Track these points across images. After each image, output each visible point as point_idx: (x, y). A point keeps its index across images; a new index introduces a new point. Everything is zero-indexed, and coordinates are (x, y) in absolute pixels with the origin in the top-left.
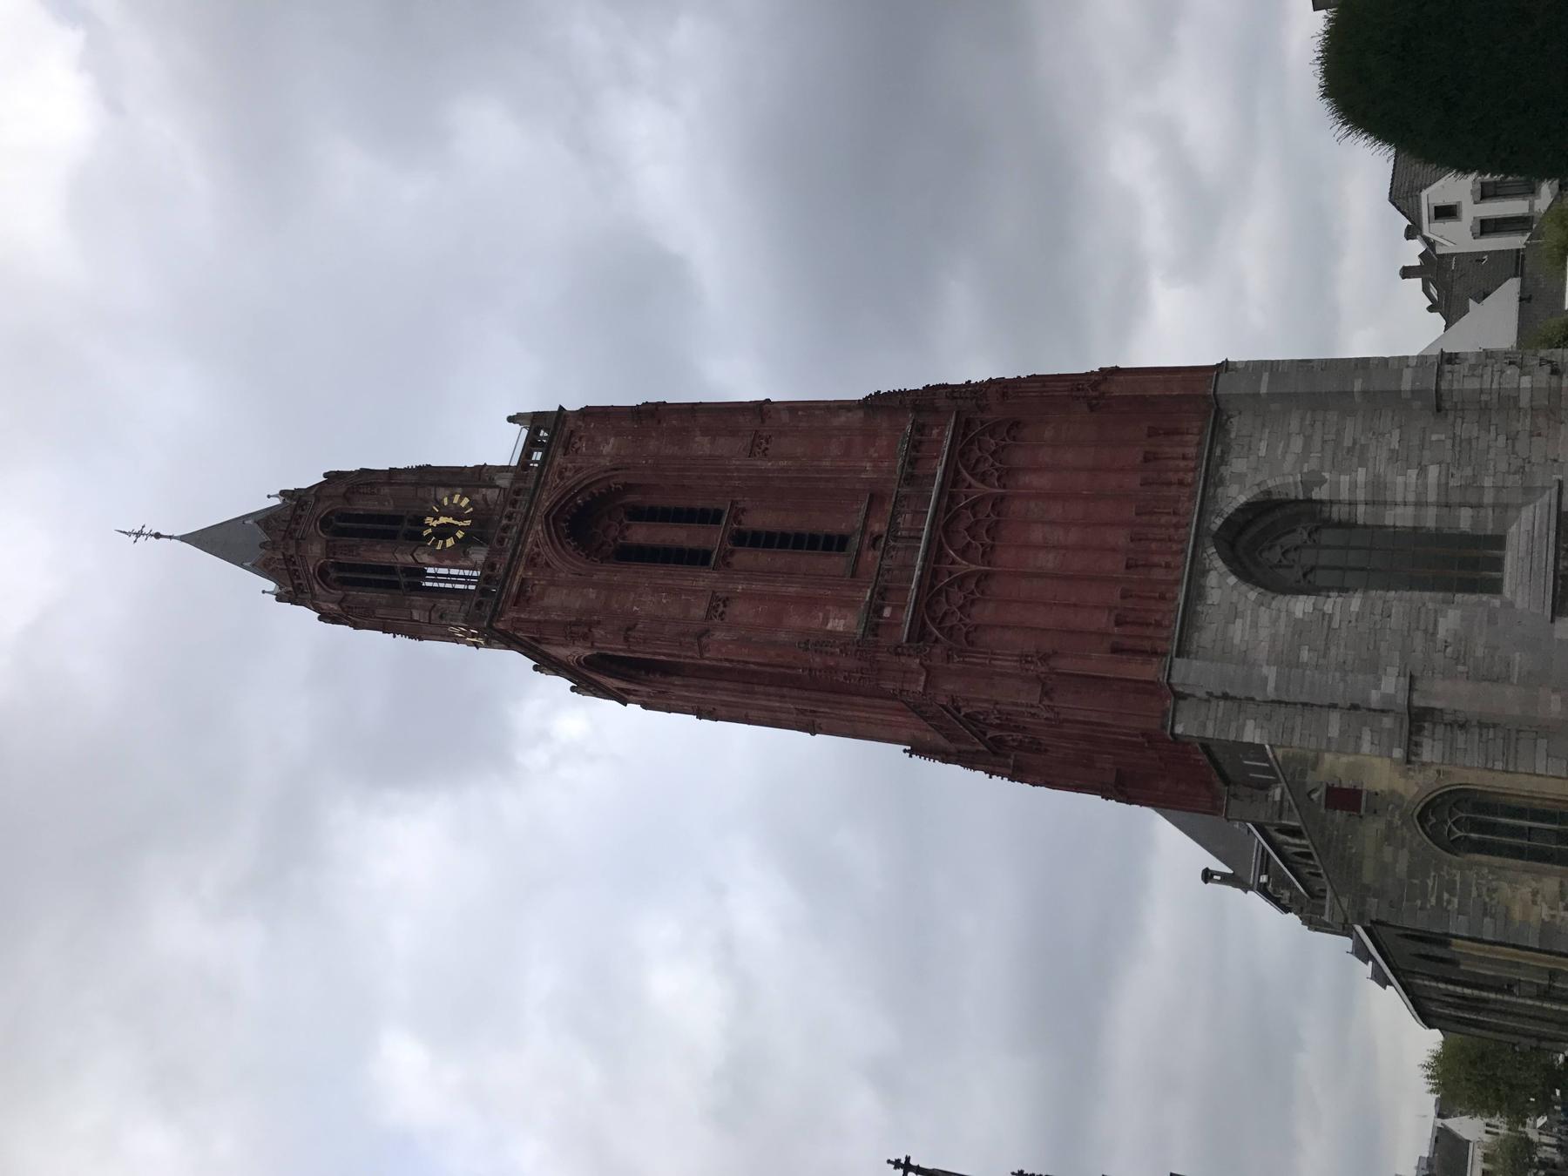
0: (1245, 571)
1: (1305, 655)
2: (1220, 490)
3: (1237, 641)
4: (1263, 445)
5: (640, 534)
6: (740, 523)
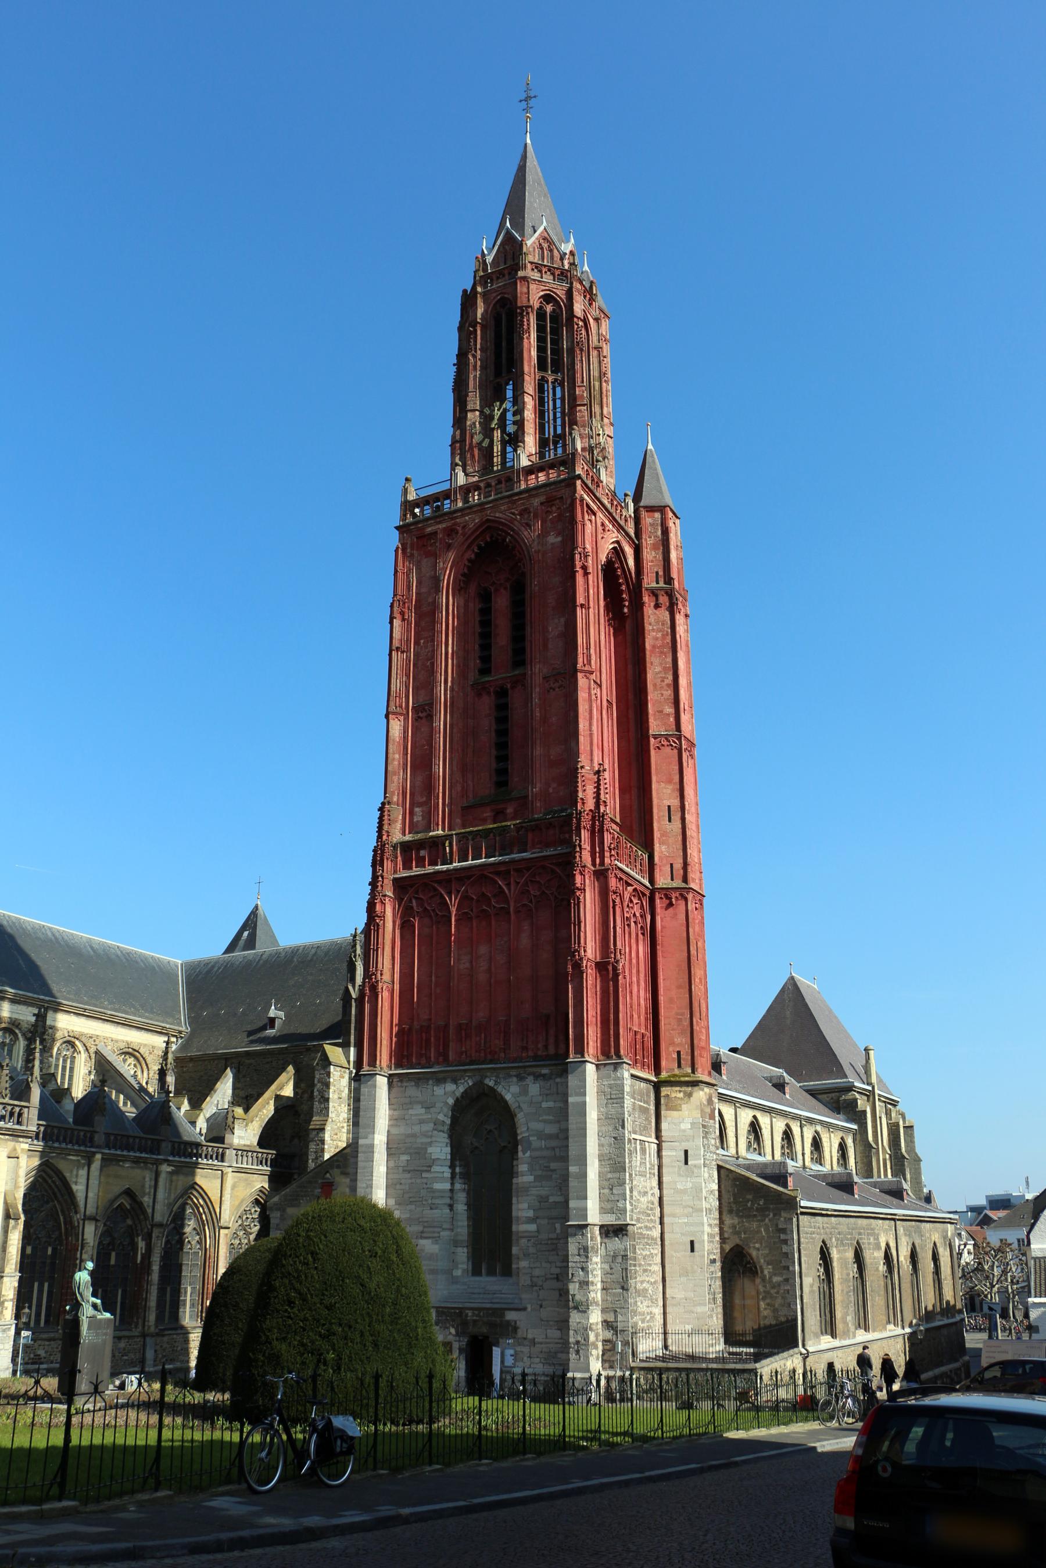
0: (460, 1108)
1: (404, 1158)
2: (515, 1079)
3: (411, 1112)
4: (551, 1104)
6: (513, 688)
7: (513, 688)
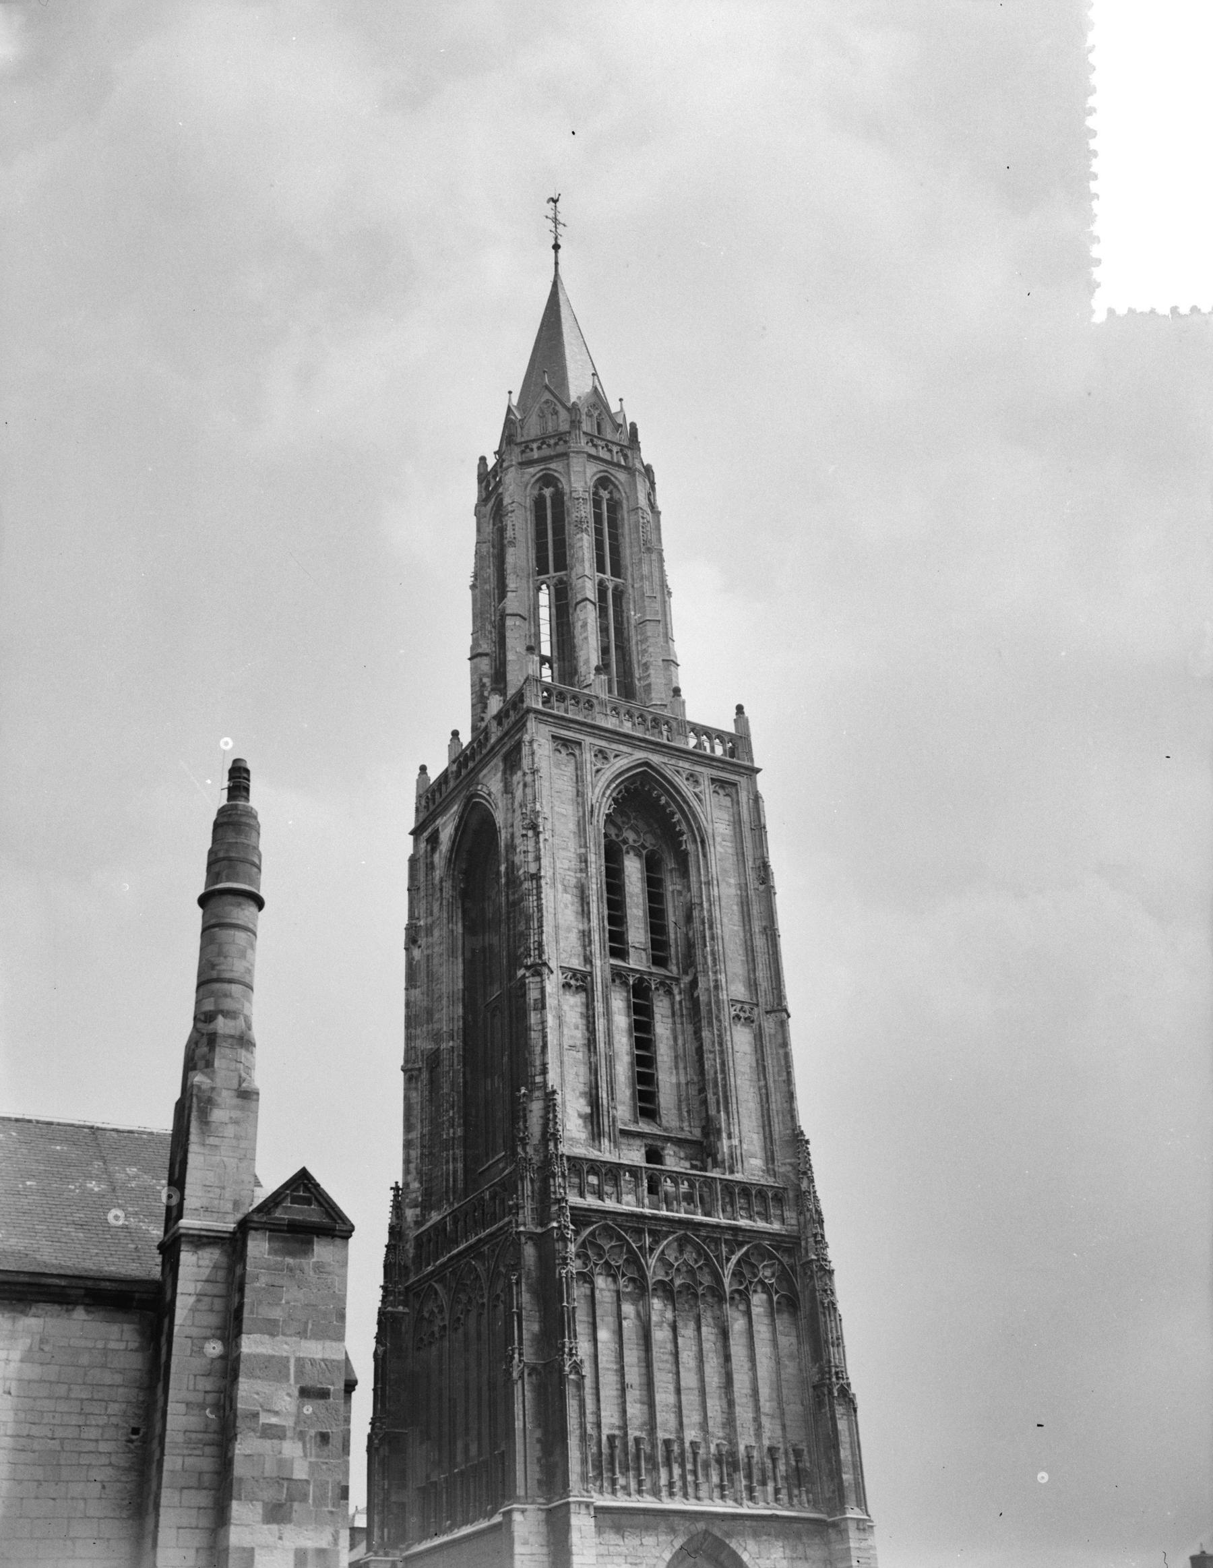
5: (633, 869)
7: (657, 989)
